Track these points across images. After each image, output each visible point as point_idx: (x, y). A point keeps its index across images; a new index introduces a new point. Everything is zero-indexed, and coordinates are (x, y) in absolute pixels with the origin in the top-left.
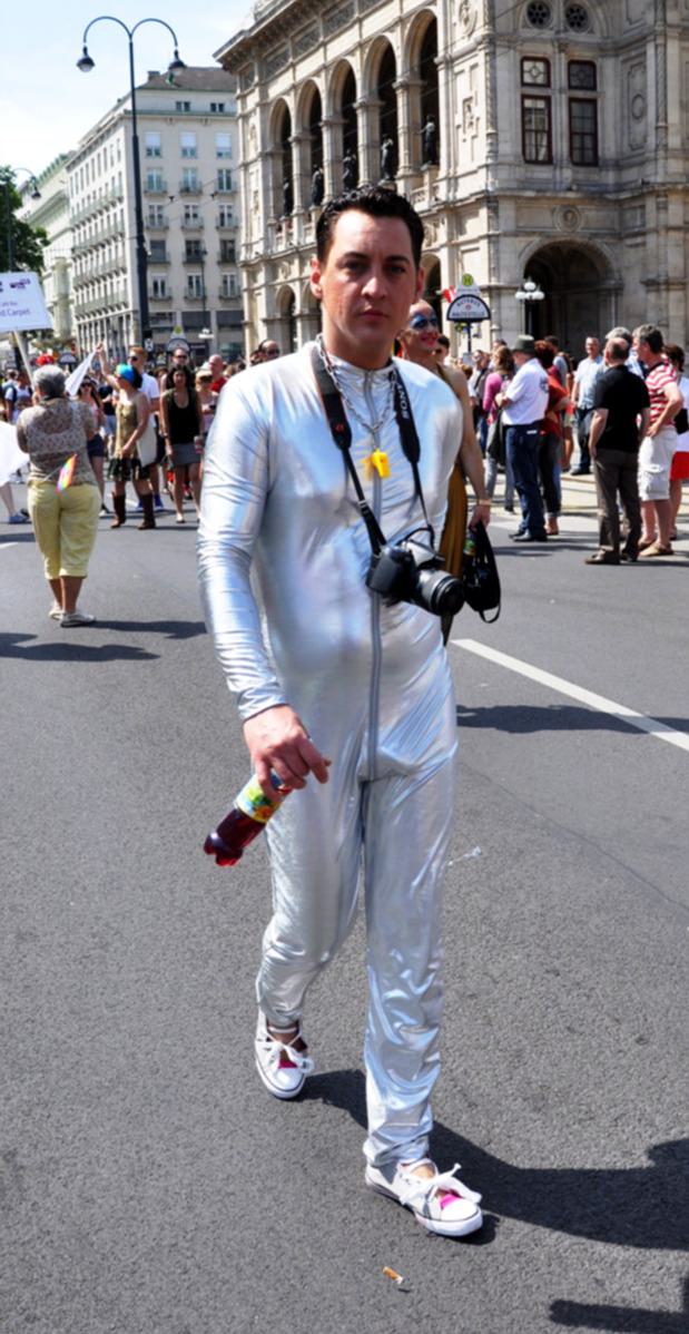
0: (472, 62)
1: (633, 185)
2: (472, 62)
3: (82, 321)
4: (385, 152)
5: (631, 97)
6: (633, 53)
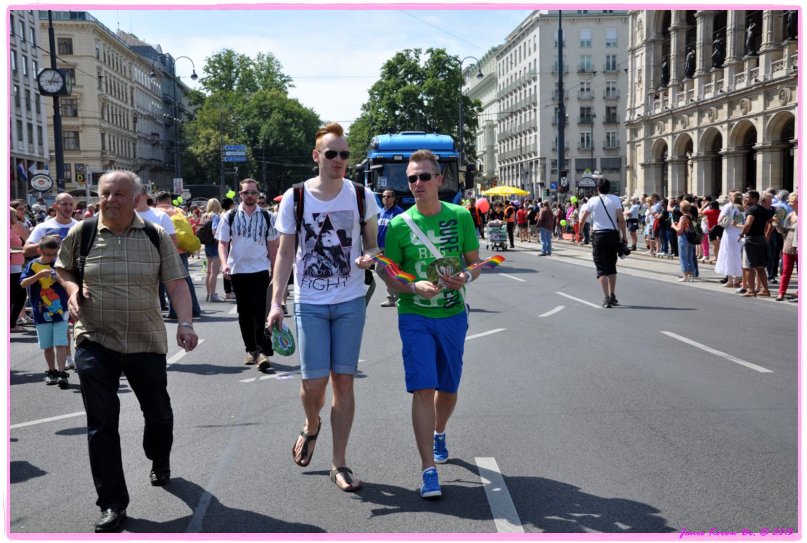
3: (503, 165)
4: (750, 33)
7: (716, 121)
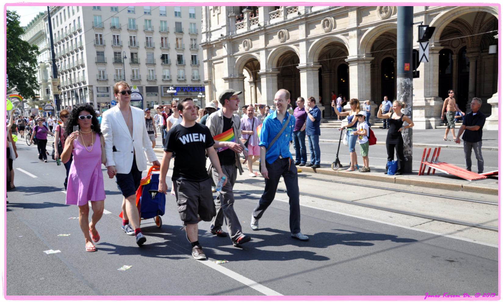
7: (334, 31)
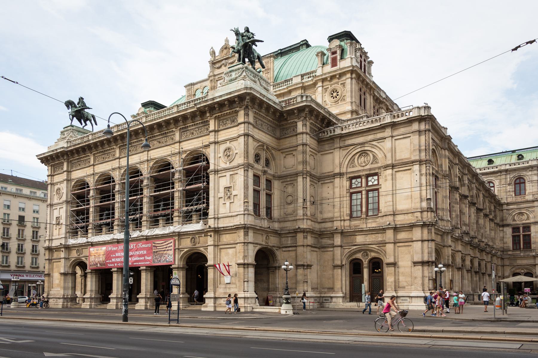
0: (232, 173)
1: (288, 228)
2: (232, 173)
5: (286, 195)
6: (288, 180)
